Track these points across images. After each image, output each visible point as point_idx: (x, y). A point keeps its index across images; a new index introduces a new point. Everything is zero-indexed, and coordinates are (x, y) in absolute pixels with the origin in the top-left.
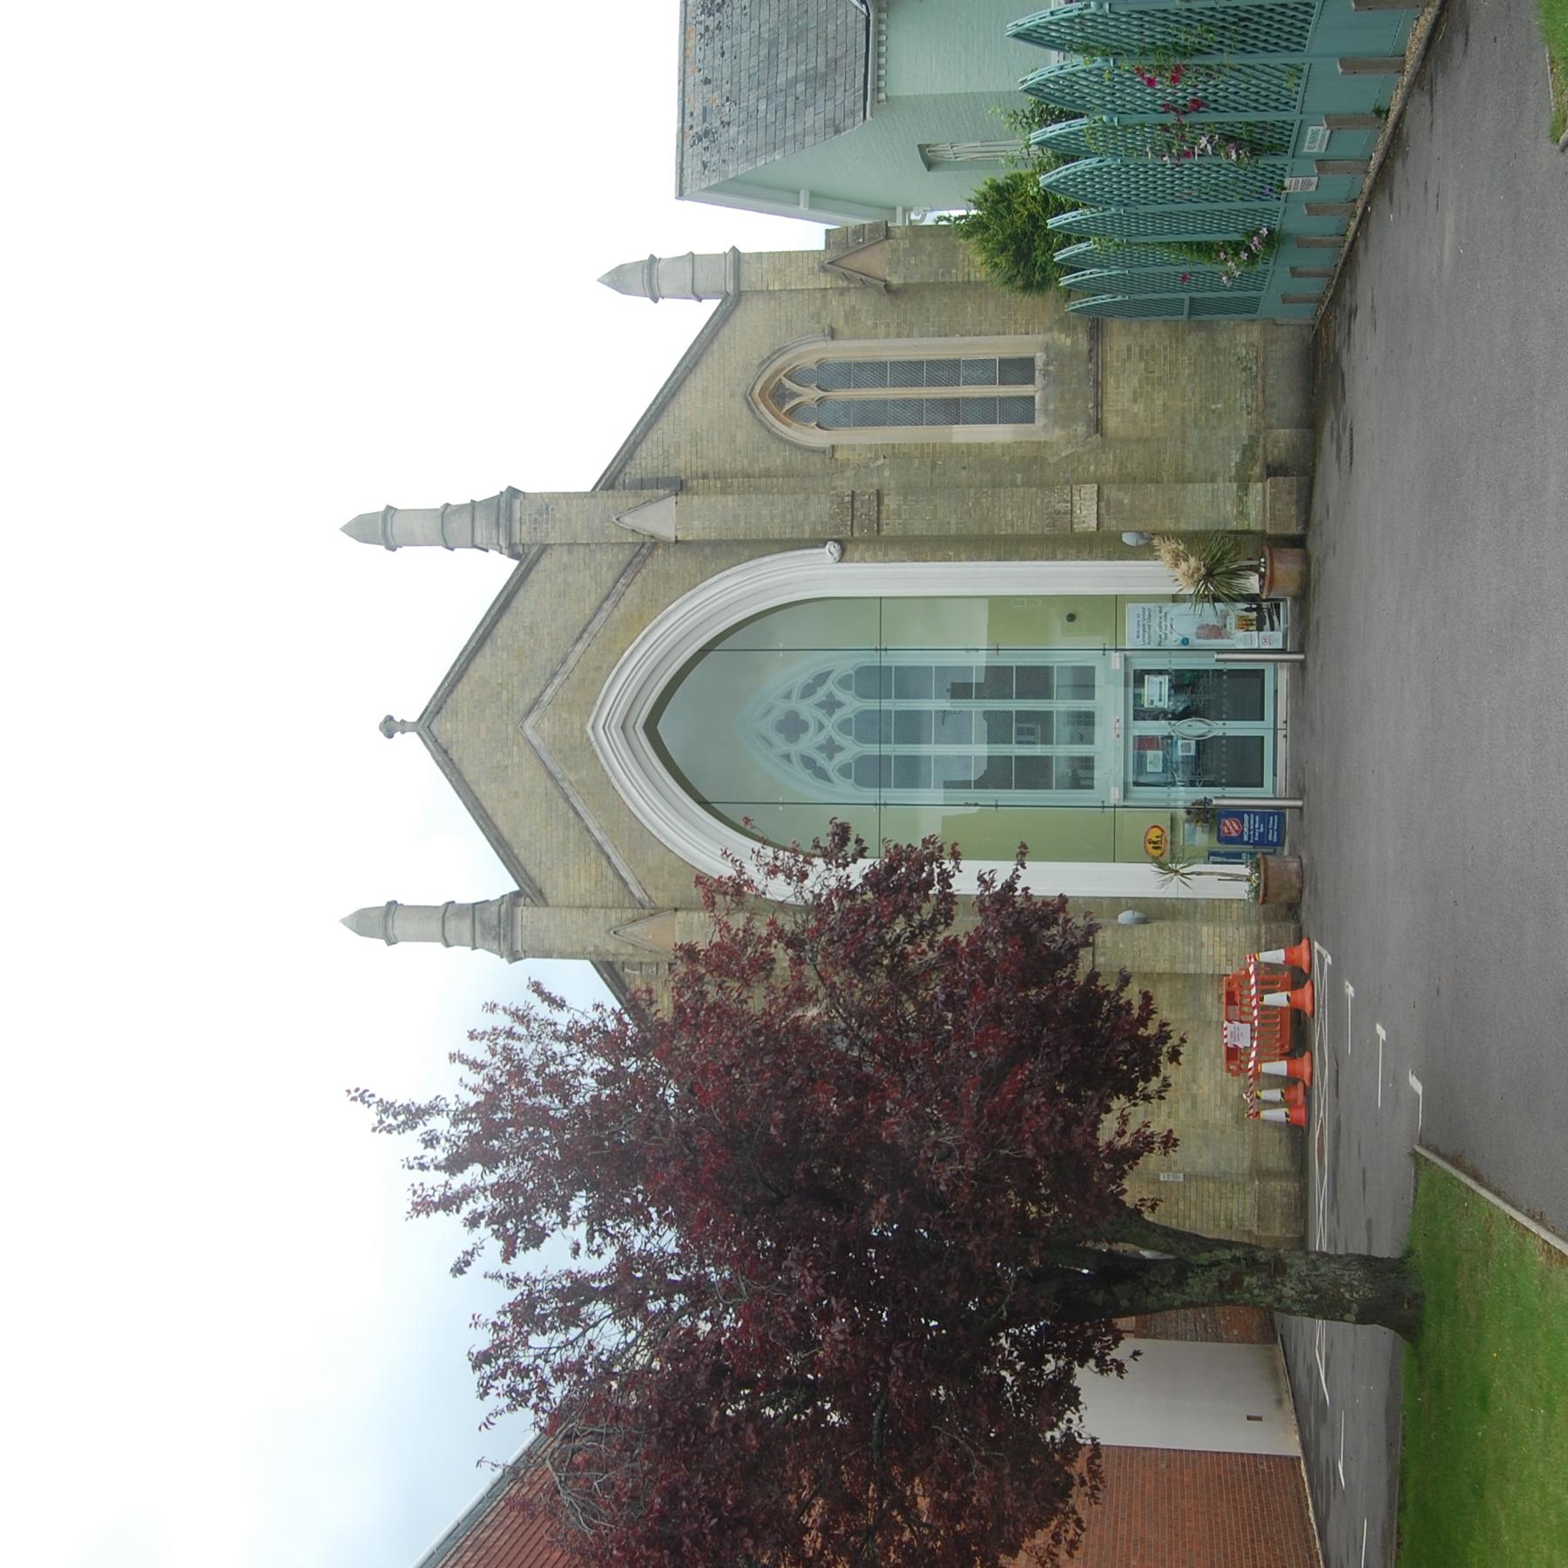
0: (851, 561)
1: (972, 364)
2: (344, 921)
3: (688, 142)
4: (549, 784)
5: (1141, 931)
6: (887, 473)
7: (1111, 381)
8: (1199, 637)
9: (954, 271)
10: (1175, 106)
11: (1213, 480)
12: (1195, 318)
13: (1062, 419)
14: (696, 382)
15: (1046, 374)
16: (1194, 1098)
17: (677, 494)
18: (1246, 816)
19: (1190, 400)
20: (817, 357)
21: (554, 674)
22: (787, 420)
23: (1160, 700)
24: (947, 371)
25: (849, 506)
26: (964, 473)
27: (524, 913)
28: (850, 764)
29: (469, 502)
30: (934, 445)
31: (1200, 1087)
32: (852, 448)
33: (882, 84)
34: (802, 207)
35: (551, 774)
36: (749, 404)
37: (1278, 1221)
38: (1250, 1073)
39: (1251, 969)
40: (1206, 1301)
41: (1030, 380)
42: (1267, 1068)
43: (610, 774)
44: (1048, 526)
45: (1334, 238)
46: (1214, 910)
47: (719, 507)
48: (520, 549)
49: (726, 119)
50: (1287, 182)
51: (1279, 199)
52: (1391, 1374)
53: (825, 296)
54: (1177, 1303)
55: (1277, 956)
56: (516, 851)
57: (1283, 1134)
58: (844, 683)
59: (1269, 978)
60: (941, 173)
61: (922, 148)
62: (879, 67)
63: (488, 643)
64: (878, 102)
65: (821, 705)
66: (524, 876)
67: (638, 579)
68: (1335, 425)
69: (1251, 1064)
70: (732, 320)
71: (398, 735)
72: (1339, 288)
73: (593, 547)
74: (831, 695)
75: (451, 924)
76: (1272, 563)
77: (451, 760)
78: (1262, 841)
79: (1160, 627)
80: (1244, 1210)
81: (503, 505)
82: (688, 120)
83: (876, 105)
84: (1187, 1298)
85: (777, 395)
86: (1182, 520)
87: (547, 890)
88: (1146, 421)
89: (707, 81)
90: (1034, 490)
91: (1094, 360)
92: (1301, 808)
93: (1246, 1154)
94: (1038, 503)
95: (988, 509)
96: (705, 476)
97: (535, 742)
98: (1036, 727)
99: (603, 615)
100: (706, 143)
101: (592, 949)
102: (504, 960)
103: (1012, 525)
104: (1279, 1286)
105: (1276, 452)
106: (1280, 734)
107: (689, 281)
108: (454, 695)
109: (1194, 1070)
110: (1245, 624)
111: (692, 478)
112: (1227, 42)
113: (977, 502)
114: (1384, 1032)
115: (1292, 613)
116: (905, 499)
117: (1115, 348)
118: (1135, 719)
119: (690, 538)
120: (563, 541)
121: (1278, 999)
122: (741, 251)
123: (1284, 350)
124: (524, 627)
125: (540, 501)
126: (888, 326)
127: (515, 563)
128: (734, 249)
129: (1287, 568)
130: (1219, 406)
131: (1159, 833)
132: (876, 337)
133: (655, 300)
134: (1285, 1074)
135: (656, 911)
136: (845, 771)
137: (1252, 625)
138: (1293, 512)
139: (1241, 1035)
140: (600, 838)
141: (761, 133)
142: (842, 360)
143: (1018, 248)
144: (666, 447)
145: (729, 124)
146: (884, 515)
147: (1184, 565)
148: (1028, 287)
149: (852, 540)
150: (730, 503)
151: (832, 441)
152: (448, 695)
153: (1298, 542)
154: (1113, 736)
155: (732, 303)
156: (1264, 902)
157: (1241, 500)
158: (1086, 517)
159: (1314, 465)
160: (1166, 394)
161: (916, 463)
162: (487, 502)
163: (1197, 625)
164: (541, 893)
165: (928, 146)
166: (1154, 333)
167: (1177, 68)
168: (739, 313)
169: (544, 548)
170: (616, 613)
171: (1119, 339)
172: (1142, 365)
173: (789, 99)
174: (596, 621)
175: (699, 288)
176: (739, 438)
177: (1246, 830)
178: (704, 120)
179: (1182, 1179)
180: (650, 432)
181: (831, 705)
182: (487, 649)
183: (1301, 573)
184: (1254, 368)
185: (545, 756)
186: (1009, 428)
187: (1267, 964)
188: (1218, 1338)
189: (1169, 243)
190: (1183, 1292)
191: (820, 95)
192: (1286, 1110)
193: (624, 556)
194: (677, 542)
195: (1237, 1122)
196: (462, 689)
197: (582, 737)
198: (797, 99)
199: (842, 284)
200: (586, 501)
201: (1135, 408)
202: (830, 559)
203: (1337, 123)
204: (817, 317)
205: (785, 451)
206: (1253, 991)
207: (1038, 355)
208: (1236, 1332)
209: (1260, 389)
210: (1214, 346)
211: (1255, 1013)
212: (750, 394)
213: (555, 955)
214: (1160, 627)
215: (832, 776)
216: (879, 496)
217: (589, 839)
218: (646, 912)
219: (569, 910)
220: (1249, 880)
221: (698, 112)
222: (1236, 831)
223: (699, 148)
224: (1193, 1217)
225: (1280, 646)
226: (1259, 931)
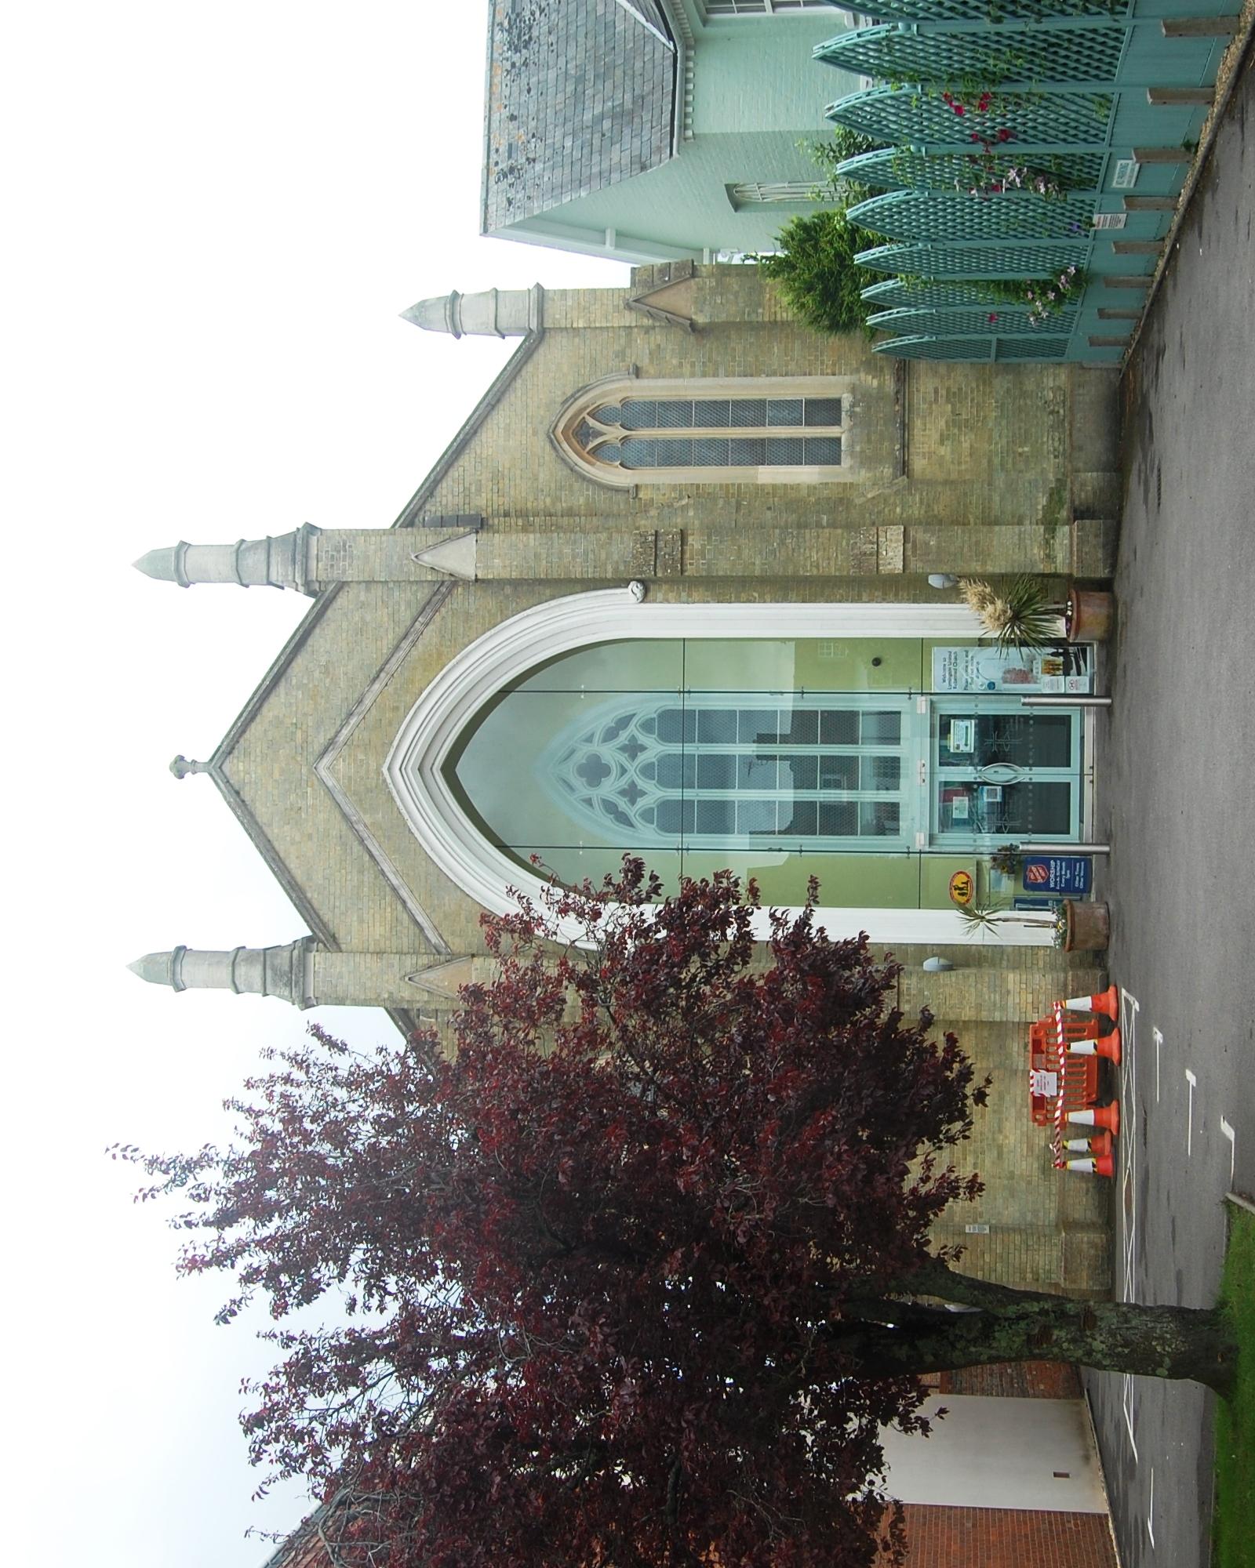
0: (654, 601)
1: (777, 404)
2: (131, 967)
3: (493, 179)
4: (344, 827)
5: (945, 978)
6: (691, 513)
7: (918, 423)
8: (1005, 682)
9: (760, 311)
10: (983, 136)
11: (1020, 523)
12: (1003, 360)
13: (867, 460)
14: (500, 418)
15: (852, 415)
16: (1000, 1148)
17: (477, 532)
18: (1052, 862)
19: (996, 444)
20: (620, 396)
21: (350, 715)
22: (591, 459)
24: (753, 411)
25: (652, 545)
26: (769, 514)
27: (317, 959)
28: (653, 809)
29: (265, 538)
30: (739, 485)
31: (1006, 1137)
32: (656, 487)
33: (689, 121)
34: (609, 247)
35: (345, 816)
36: (551, 442)
37: (1084, 1274)
38: (1057, 1123)
39: (1058, 1017)
40: (1014, 1355)
41: (837, 422)
42: (1074, 1117)
43: (406, 817)
44: (853, 567)
45: (1142, 279)
46: (1020, 957)
47: (521, 546)
48: (316, 587)
49: (531, 156)
50: (1095, 218)
51: (1087, 236)
52: (1202, 1430)
53: (629, 335)
54: (984, 1357)
55: (1084, 1003)
56: (309, 895)
58: (647, 726)
59: (1076, 1026)
60: (748, 214)
61: (729, 188)
62: (686, 104)
63: (283, 683)
64: (685, 139)
65: (623, 749)
66: (317, 921)
67: (437, 617)
68: (1143, 467)
69: (1058, 1114)
70: (535, 356)
71: (188, 775)
72: (1147, 330)
73: (391, 585)
74: (633, 738)
75: (242, 970)
76: (1079, 606)
77: (243, 801)
78: (1069, 888)
81: (299, 541)
82: (494, 157)
83: (683, 143)
84: (993, 1352)
85: (580, 433)
86: (989, 562)
87: (341, 935)
88: (953, 462)
89: (513, 118)
90: (839, 531)
91: (901, 402)
92: (1107, 854)
94: (844, 543)
95: (793, 550)
96: (506, 514)
97: (330, 784)
98: (842, 771)
99: (400, 654)
100: (511, 179)
101: (386, 996)
102: (296, 1006)
103: (817, 567)
104: (1089, 1340)
105: (1083, 495)
106: (1087, 779)
107: (492, 318)
108: (247, 735)
109: (1000, 1121)
110: (1051, 669)
111: (493, 516)
112: (1037, 69)
113: (782, 543)
114: (1194, 1078)
115: (1098, 657)
116: (709, 537)
117: (922, 389)
118: (941, 764)
119: (490, 576)
120: (361, 579)
121: (1085, 1047)
122: (546, 288)
123: (1092, 393)
124: (320, 666)
125: (337, 538)
126: (693, 365)
127: (312, 600)
128: (538, 286)
129: (1094, 612)
130: (1026, 449)
131: (965, 879)
132: (681, 376)
133: (458, 336)
134: (1092, 1123)
135: (452, 957)
136: (647, 815)
137: (1059, 669)
138: (1100, 556)
139: (1047, 1084)
140: (395, 882)
141: (567, 170)
142: (647, 399)
143: (825, 288)
144: (467, 485)
145: (534, 160)
146: (687, 555)
147: (990, 608)
148: (835, 326)
149: (656, 581)
150: (532, 542)
151: (637, 481)
152: (240, 736)
154: (919, 781)
155: (536, 339)
156: (1070, 949)
157: (1047, 542)
158: (893, 558)
159: (1121, 508)
161: (721, 502)
162: (283, 539)
164: (334, 937)
165: (735, 186)
166: (961, 375)
167: (986, 96)
168: (541, 350)
169: (342, 586)
170: (414, 652)
171: (926, 383)
173: (596, 136)
174: (394, 660)
175: (502, 325)
176: (541, 476)
177: (1052, 876)
178: (510, 157)
179: (987, 1231)
180: (451, 470)
181: (633, 749)
182: (282, 688)
183: (1108, 617)
184: (1062, 411)
185: (340, 798)
186: (815, 469)
187: (1074, 1012)
188: (1024, 1394)
189: (977, 281)
190: (990, 1347)
191: (627, 131)
192: (1093, 1160)
193: (423, 594)
194: (477, 580)
196: (255, 729)
197: (378, 779)
198: (603, 135)
199: (646, 322)
200: (384, 538)
201: (942, 451)
202: (633, 599)
203: (1146, 156)
204: (621, 355)
205: (588, 490)
206: (1060, 1039)
207: (845, 396)
208: (1042, 1387)
210: (1021, 389)
211: (1062, 1061)
212: (553, 432)
213: (348, 1002)
215: (634, 820)
216: (683, 535)
217: (384, 883)
218: (442, 958)
219: (363, 955)
220: (1055, 927)
221: (503, 149)
223: (504, 184)
225: (1087, 691)
226: (1066, 978)
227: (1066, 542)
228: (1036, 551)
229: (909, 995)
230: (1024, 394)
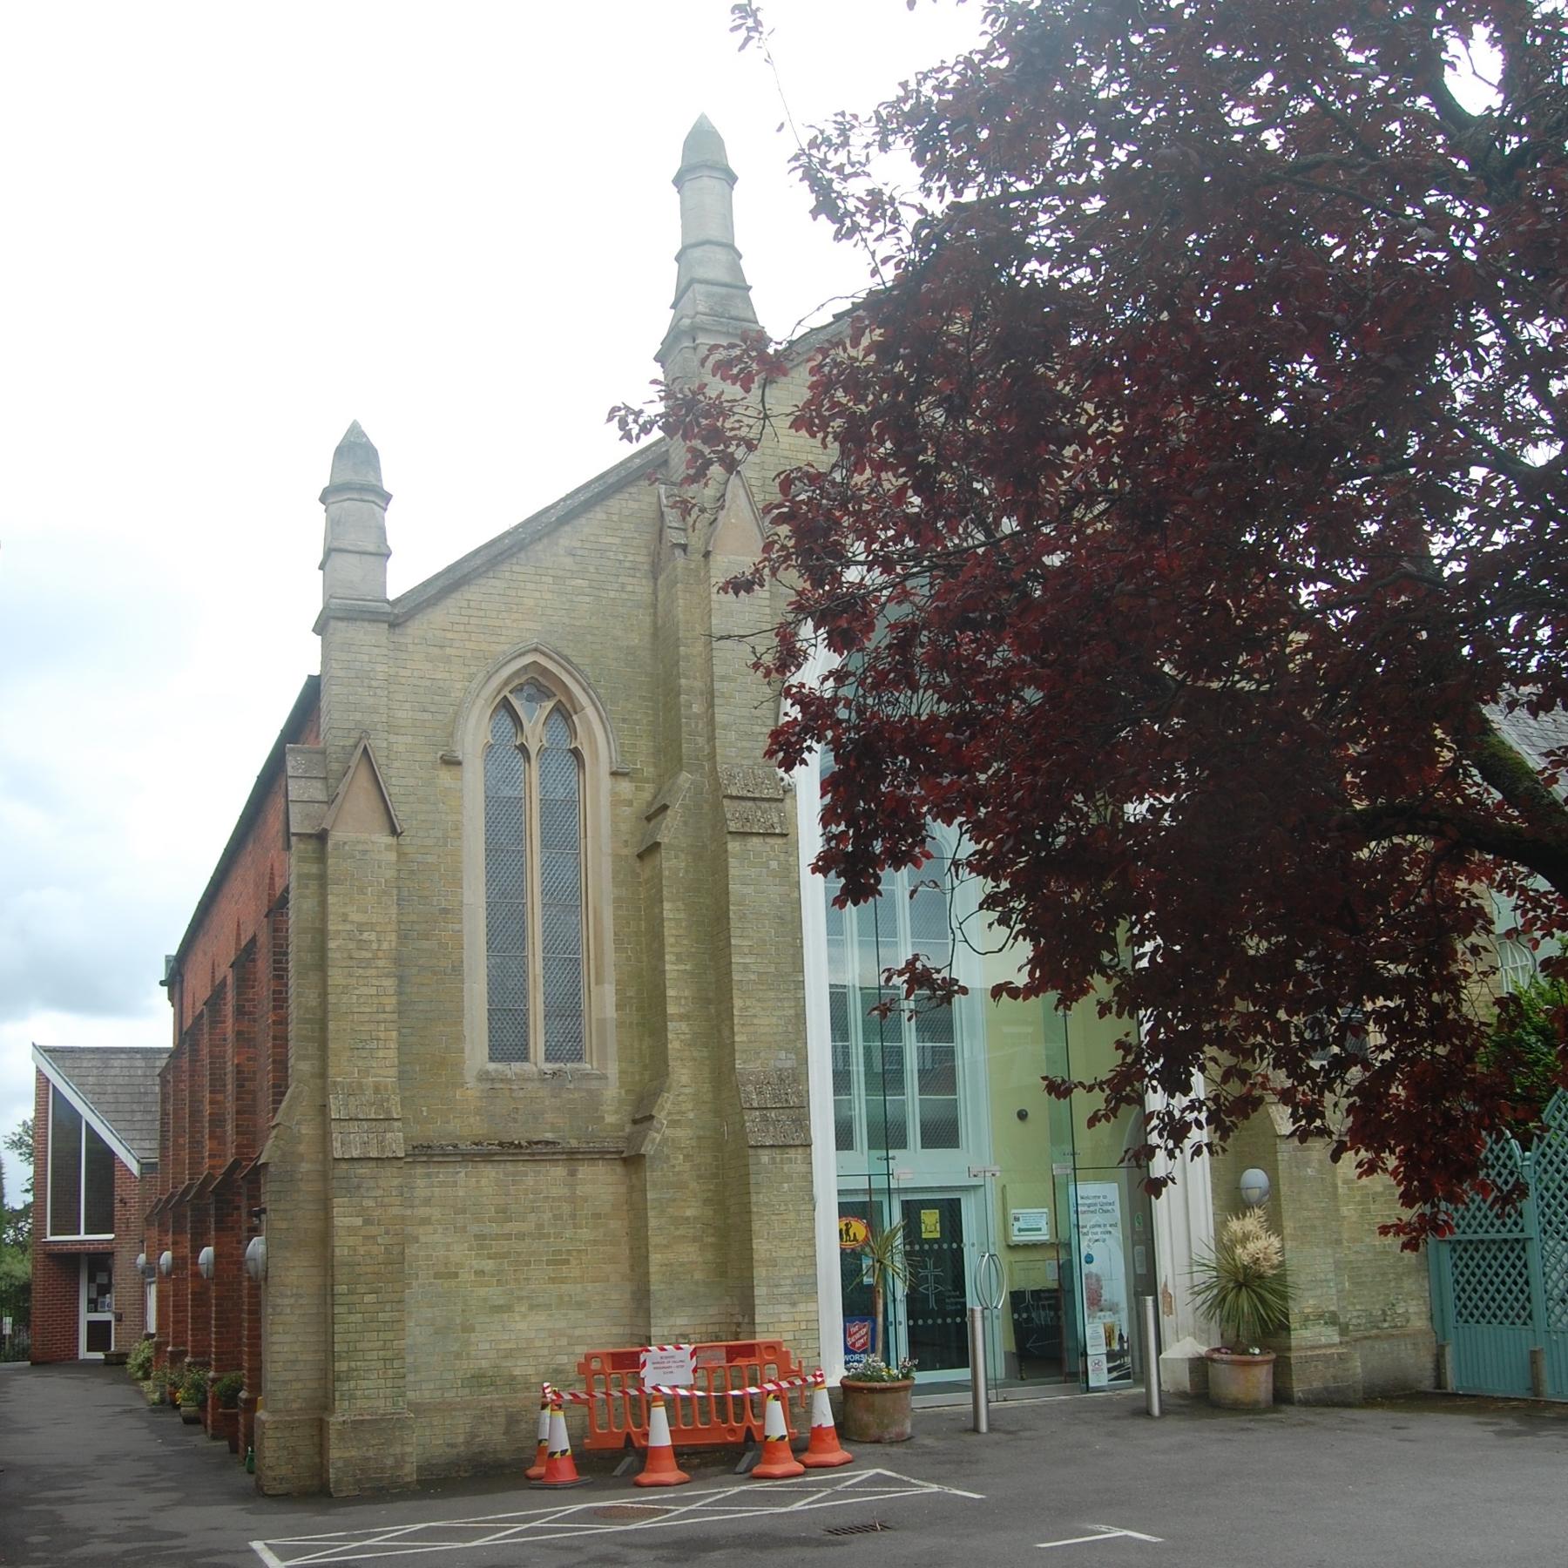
16: (507, 1308)
19: (1349, 1248)
23: (1020, 1230)
31: (524, 1316)
57: (462, 1448)
59: (797, 1409)
79: (1094, 1226)
80: (368, 1398)
86: (1294, 1244)
92: (976, 1430)
109: (548, 1306)
121: (776, 1424)
153: (1281, 1397)
157: (1321, 1316)
160: (1354, 1219)
163: (1099, 1273)
172: (1380, 1189)
183: (1257, 1402)
184: (1386, 1325)
195: (473, 1377)
209: (1367, 1334)
210: (1404, 1274)
214: (1094, 1226)
222: (854, 1344)
224: (352, 1318)
225: (1091, 1384)
227: (1323, 1340)
228: (1311, 1302)
229: (782, 1161)
230: (1399, 1278)
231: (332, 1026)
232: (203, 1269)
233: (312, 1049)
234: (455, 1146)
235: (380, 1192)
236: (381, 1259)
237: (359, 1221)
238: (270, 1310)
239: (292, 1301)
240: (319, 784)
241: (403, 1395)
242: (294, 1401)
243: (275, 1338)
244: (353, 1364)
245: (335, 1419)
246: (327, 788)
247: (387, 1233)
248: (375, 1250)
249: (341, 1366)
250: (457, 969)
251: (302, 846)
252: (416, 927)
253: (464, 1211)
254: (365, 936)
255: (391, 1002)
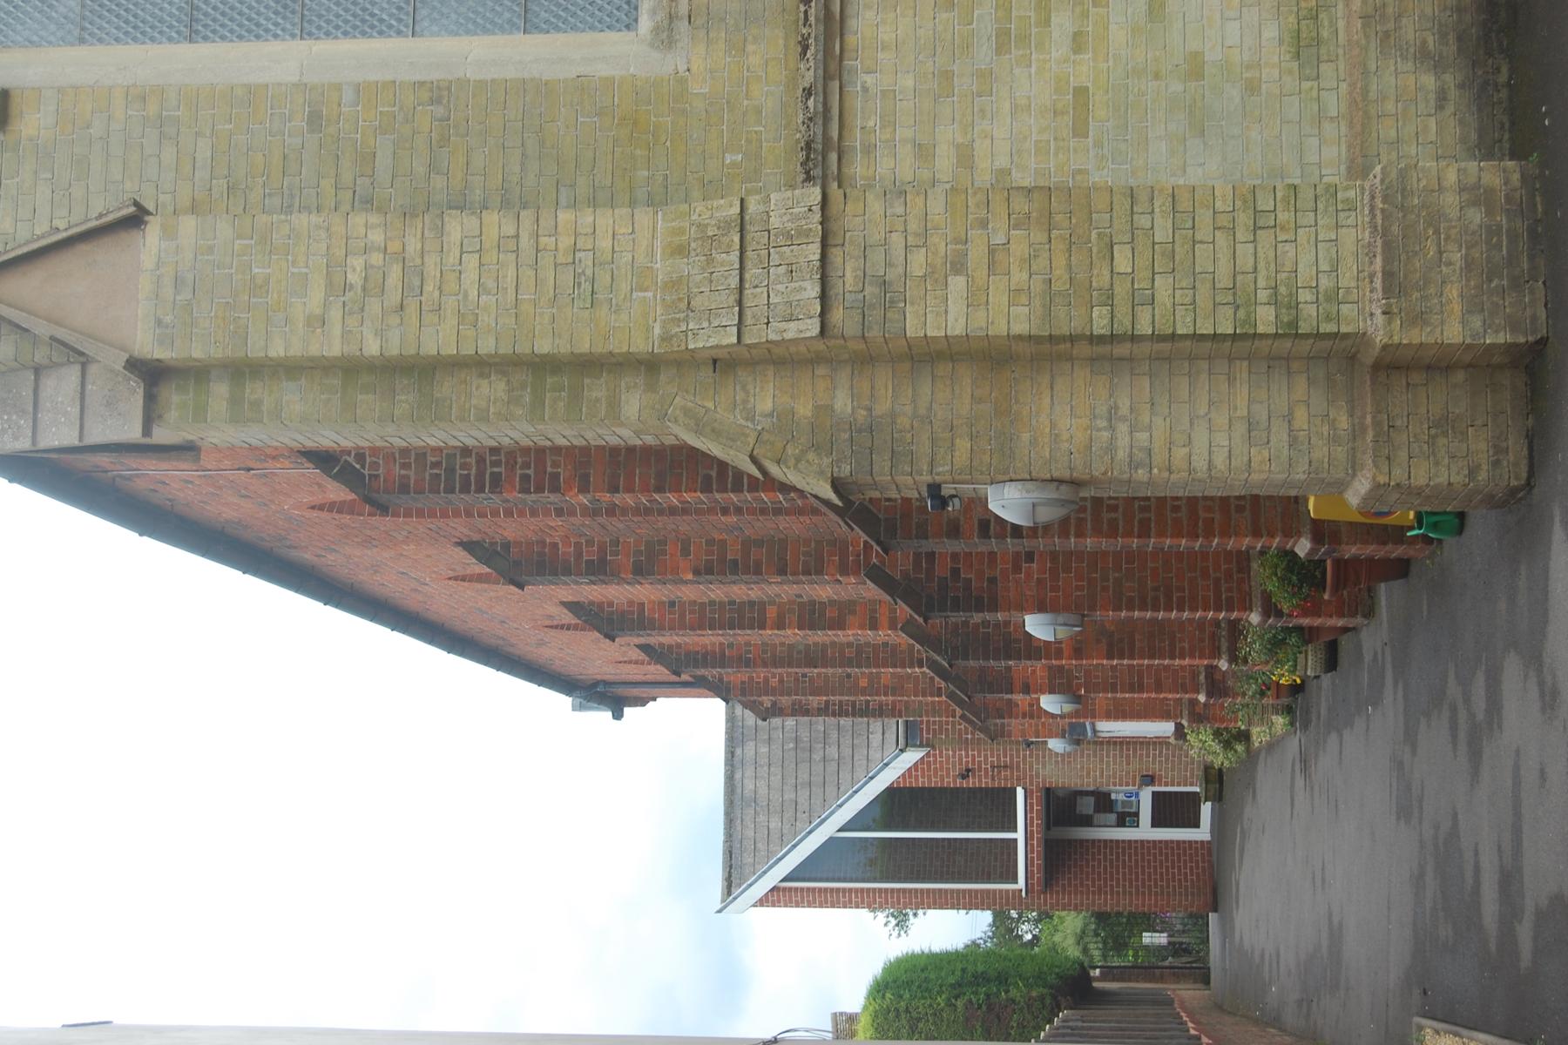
37: (1453, 292)
57: (1448, 77)
93: (1331, 152)
195: (1298, 56)
231: (544, 346)
232: (1063, 633)
233: (597, 389)
234: (808, 92)
235: (897, 238)
236: (1039, 236)
237: (957, 283)
238: (1141, 474)
239: (1123, 428)
240: (49, 384)
241: (1333, 191)
242: (1333, 424)
243: (1200, 464)
244: (1263, 295)
245: (1379, 330)
246: (54, 366)
247: (984, 224)
248: (1019, 248)
249: (1266, 318)
250: (437, 92)
251: (172, 415)
252: (347, 177)
253: (947, 76)
254: (354, 278)
255: (496, 223)
